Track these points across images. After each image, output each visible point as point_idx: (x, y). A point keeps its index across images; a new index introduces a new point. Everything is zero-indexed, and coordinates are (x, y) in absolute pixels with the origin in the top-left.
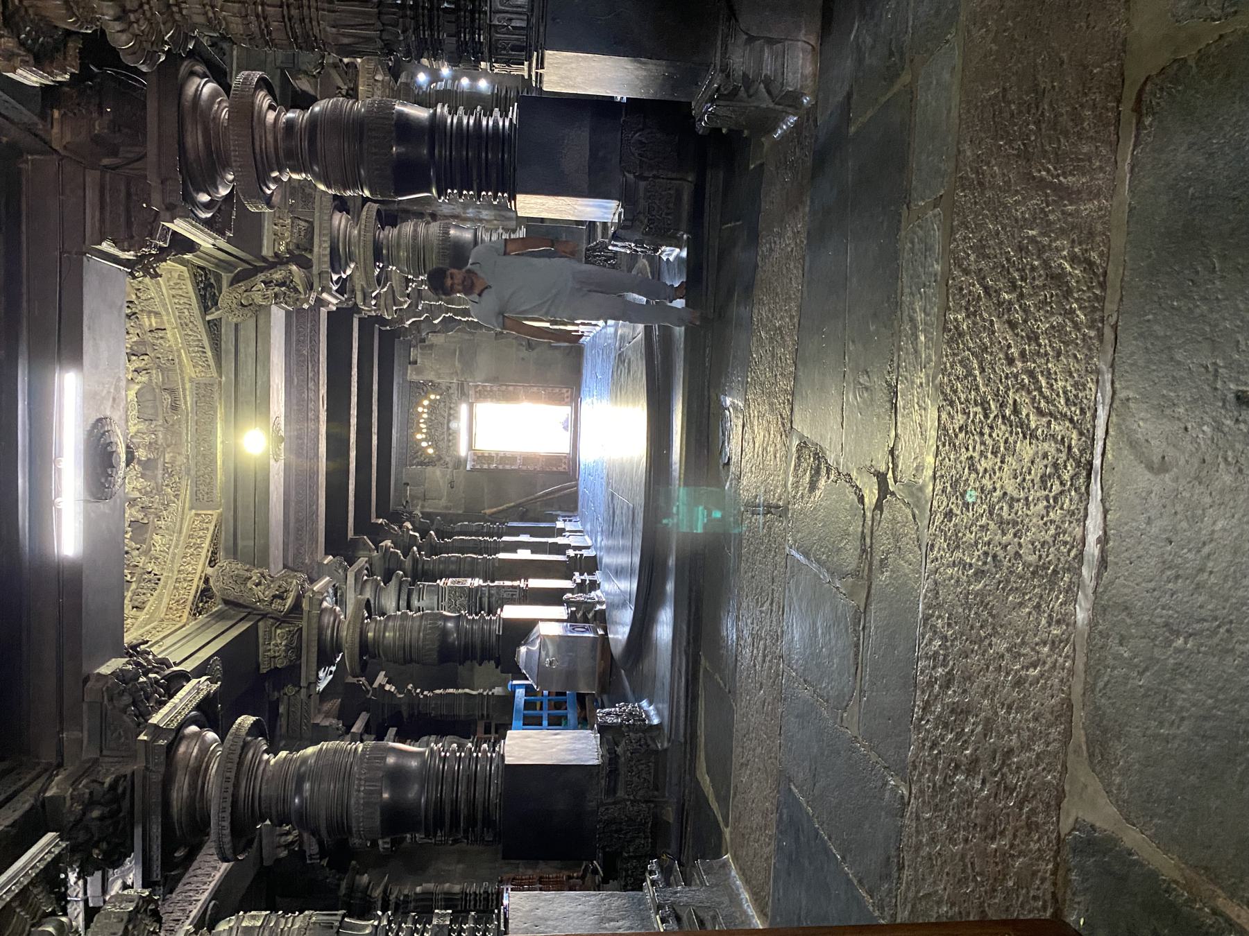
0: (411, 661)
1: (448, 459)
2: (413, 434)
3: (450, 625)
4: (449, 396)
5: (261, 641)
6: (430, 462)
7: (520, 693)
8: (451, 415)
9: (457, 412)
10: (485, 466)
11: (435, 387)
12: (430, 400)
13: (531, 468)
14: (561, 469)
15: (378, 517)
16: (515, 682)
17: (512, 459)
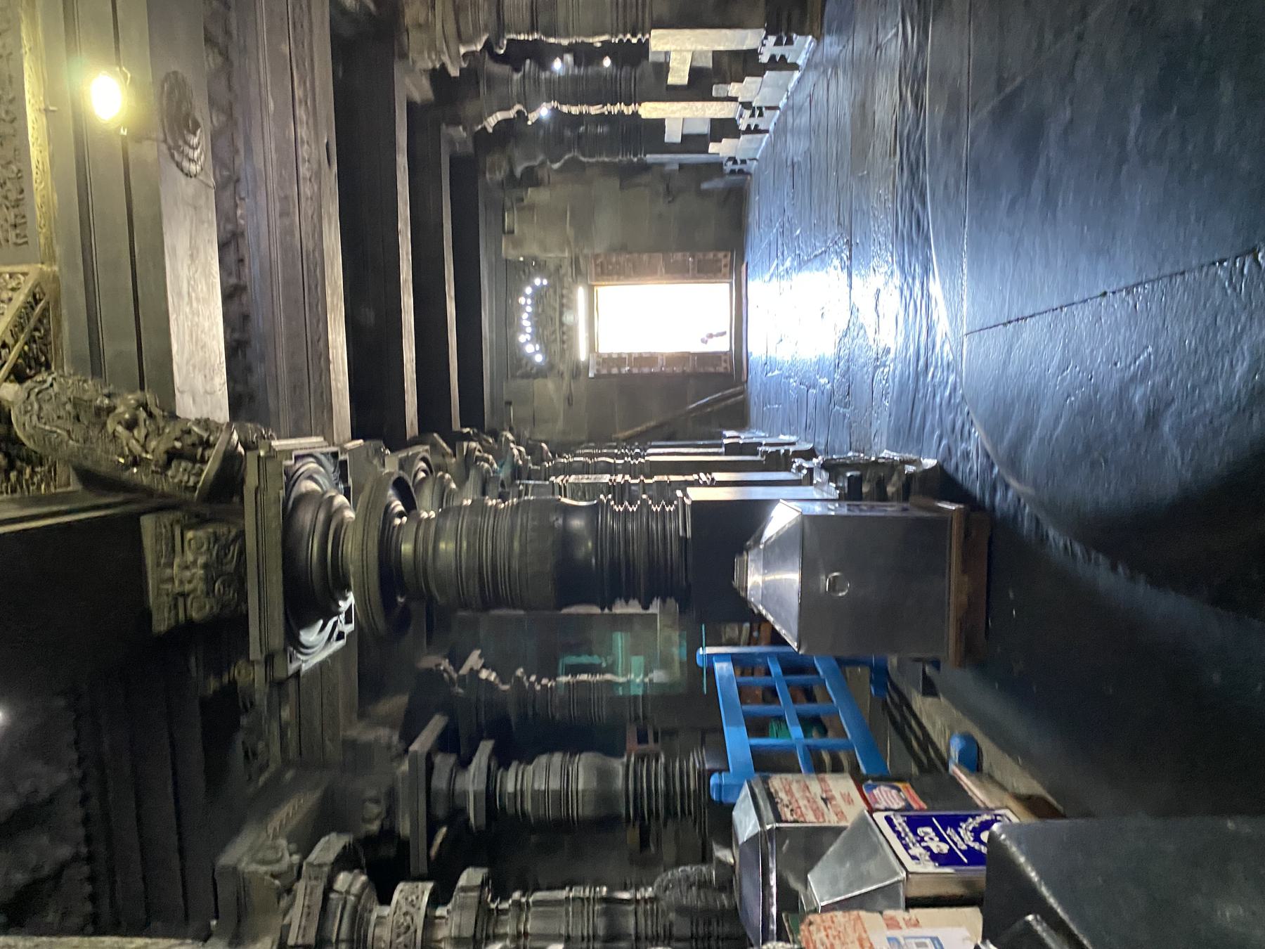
0: (499, 602)
1: (562, 367)
2: (514, 337)
3: (577, 523)
4: (561, 280)
5: (149, 560)
6: (541, 373)
7: (723, 669)
8: (565, 304)
9: (570, 300)
10: (615, 371)
11: (541, 267)
12: (534, 287)
13: (677, 369)
14: (721, 369)
15: (462, 426)
16: (709, 650)
17: (650, 359)
